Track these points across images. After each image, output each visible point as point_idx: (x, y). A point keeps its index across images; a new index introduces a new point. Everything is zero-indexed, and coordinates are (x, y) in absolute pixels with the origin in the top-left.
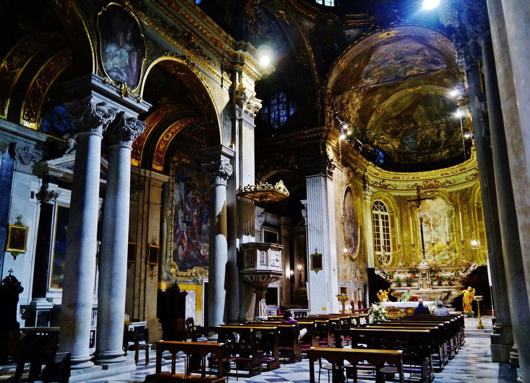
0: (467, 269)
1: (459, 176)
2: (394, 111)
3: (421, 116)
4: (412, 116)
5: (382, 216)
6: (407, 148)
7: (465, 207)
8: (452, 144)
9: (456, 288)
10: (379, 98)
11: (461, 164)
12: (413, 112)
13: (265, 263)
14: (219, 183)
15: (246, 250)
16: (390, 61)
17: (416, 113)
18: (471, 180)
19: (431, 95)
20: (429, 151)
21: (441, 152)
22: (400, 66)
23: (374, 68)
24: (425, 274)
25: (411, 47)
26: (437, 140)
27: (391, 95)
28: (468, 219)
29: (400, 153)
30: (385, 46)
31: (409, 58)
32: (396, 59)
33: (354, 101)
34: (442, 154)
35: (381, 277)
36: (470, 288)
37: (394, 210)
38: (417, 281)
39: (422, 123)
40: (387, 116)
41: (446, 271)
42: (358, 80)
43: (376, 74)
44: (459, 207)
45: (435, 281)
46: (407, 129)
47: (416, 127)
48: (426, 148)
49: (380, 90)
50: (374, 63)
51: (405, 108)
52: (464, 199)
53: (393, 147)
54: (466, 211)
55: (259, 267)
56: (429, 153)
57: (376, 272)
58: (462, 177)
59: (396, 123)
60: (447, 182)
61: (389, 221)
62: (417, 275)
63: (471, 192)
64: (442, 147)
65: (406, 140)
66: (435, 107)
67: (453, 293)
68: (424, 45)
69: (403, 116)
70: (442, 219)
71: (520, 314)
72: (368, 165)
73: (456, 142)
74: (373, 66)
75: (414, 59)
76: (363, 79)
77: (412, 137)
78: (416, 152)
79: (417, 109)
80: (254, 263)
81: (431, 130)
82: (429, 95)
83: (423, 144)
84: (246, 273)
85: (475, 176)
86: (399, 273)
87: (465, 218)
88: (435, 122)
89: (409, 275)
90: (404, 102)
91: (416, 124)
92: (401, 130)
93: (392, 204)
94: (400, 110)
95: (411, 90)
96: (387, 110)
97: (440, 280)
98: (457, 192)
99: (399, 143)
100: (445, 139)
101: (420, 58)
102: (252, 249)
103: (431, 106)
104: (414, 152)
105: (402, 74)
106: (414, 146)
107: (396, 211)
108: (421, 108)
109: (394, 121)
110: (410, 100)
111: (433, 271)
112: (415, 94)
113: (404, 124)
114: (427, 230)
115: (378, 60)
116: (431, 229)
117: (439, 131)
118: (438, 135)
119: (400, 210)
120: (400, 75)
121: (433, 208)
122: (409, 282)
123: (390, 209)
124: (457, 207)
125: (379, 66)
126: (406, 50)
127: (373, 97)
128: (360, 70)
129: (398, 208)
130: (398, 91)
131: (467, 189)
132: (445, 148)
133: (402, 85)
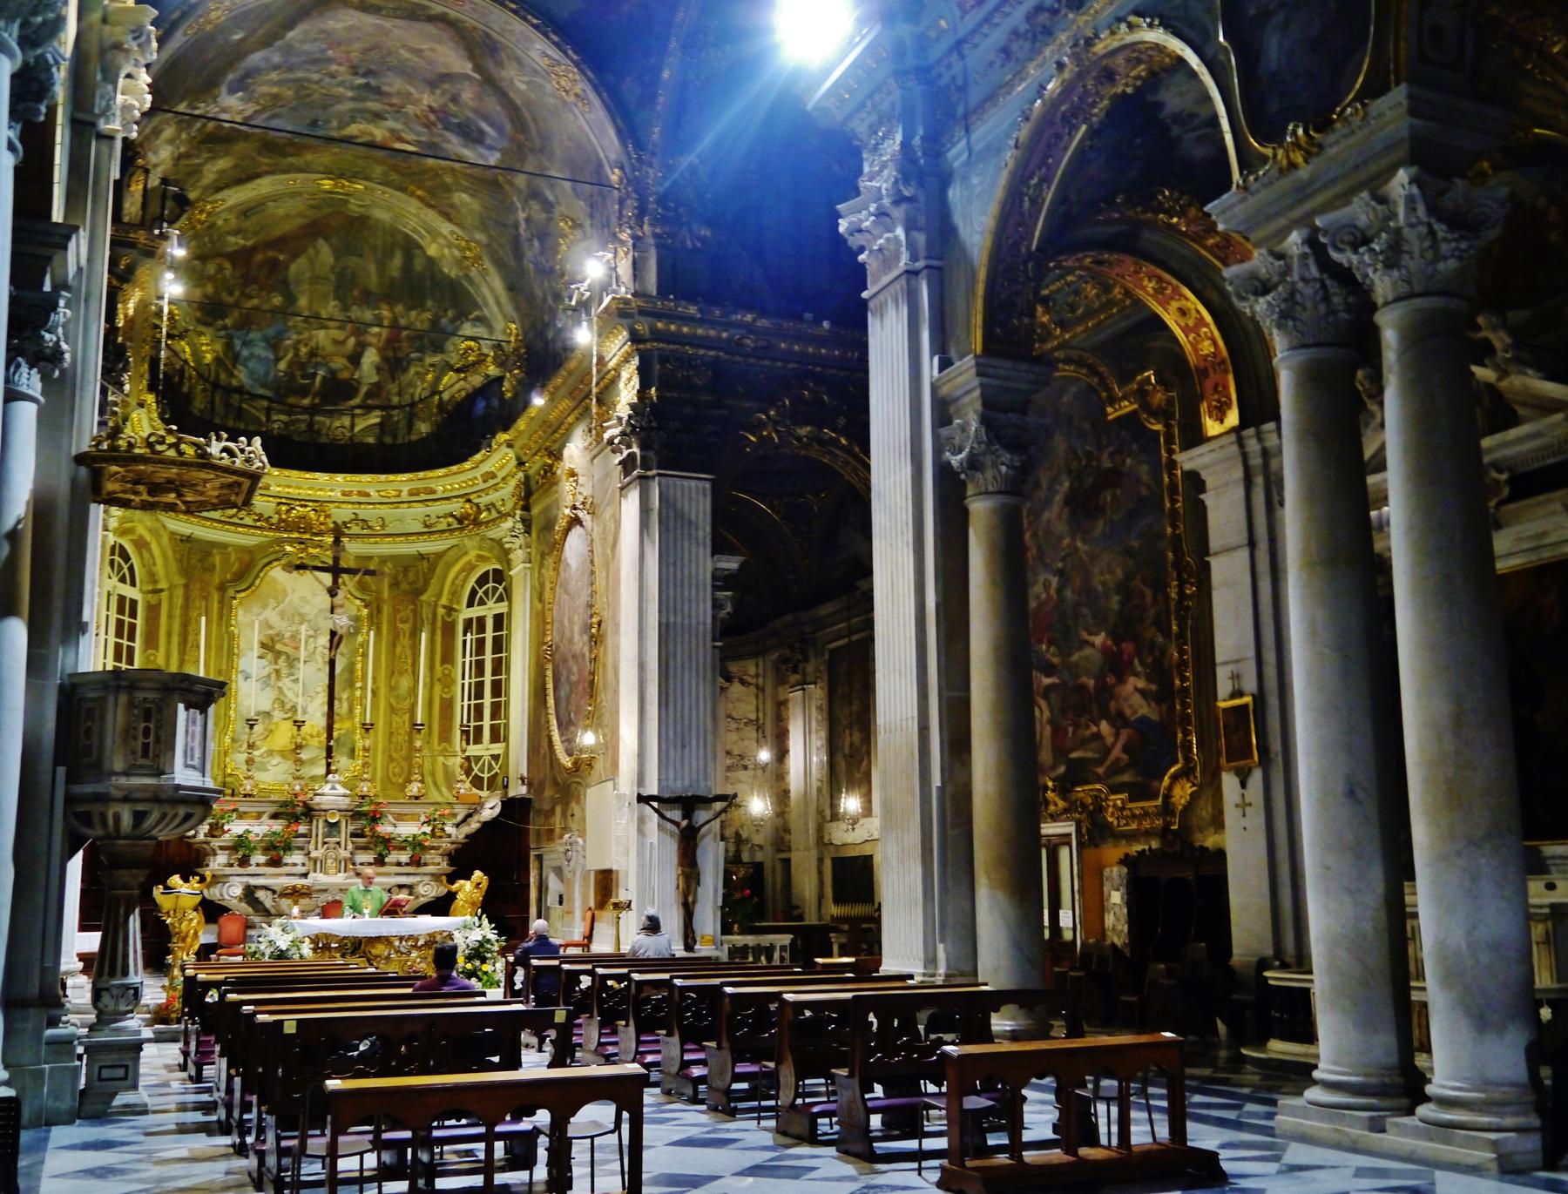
0: (470, 815)
1: (404, 510)
2: (237, 232)
3: (316, 279)
4: (287, 268)
5: (122, 599)
6: (242, 376)
7: (407, 612)
8: (395, 400)
9: (432, 875)
10: (221, 172)
11: (421, 474)
12: (295, 256)
13: (196, 762)
14: (24, 389)
15: (123, 698)
16: (334, 67)
17: (302, 262)
18: (443, 531)
19: (377, 220)
20: (313, 405)
21: (353, 416)
22: (350, 94)
23: (276, 67)
24: (336, 825)
25: (429, 54)
26: (345, 375)
27: (258, 176)
28: (409, 652)
29: (216, 385)
30: (357, 14)
31: (394, 84)
32: (354, 71)
33: (155, 153)
34: (353, 426)
36: (478, 874)
37: (163, 585)
38: (302, 848)
39: (311, 303)
40: (211, 241)
41: (400, 817)
42: (208, 87)
43: (264, 89)
44: (386, 609)
45: (365, 848)
46: (256, 308)
47: (287, 311)
48: (303, 391)
49: (240, 147)
50: (288, 50)
51: (276, 233)
52: (404, 586)
53: (196, 354)
54: (407, 627)
55: (183, 775)
56: (313, 410)
58: (412, 517)
59: (228, 273)
60: (356, 519)
61: (139, 622)
62: (302, 829)
63: (432, 569)
65: (245, 344)
66: (372, 268)
67: (421, 890)
68: (478, 68)
69: (259, 257)
71: (1474, 927)
72: (141, 405)
73: (407, 399)
74: (277, 59)
75: (409, 94)
76: (224, 89)
77: (266, 339)
78: (268, 393)
79: (311, 251)
80: (157, 756)
81: (339, 335)
82: (368, 218)
83: (298, 373)
84: (120, 794)
85: (460, 520)
86: (241, 816)
87: (399, 650)
88: (355, 312)
89: (278, 826)
90: (281, 212)
91: (291, 299)
92: (237, 305)
93: (159, 561)
94: (256, 234)
95: (327, 184)
96: (220, 222)
97: (387, 842)
99: (218, 347)
100: (375, 379)
101: (427, 99)
102: (150, 695)
103: (361, 256)
104: (261, 391)
105: (335, 123)
106: (267, 374)
107: (171, 588)
108: (324, 253)
109: (227, 265)
110: (301, 215)
111: (364, 817)
112: (329, 200)
113: (250, 290)
114: (265, 672)
115: (307, 47)
116: (277, 671)
117: (361, 347)
118: (355, 359)
119: (186, 586)
120: (328, 121)
121: (296, 600)
122: (276, 852)
123: (153, 578)
124: (379, 610)
125: (291, 69)
126: (405, 54)
127: (208, 160)
128: (240, 51)
129: (179, 581)
130: (286, 171)
131: (421, 557)
132: (368, 409)
133: (309, 157)
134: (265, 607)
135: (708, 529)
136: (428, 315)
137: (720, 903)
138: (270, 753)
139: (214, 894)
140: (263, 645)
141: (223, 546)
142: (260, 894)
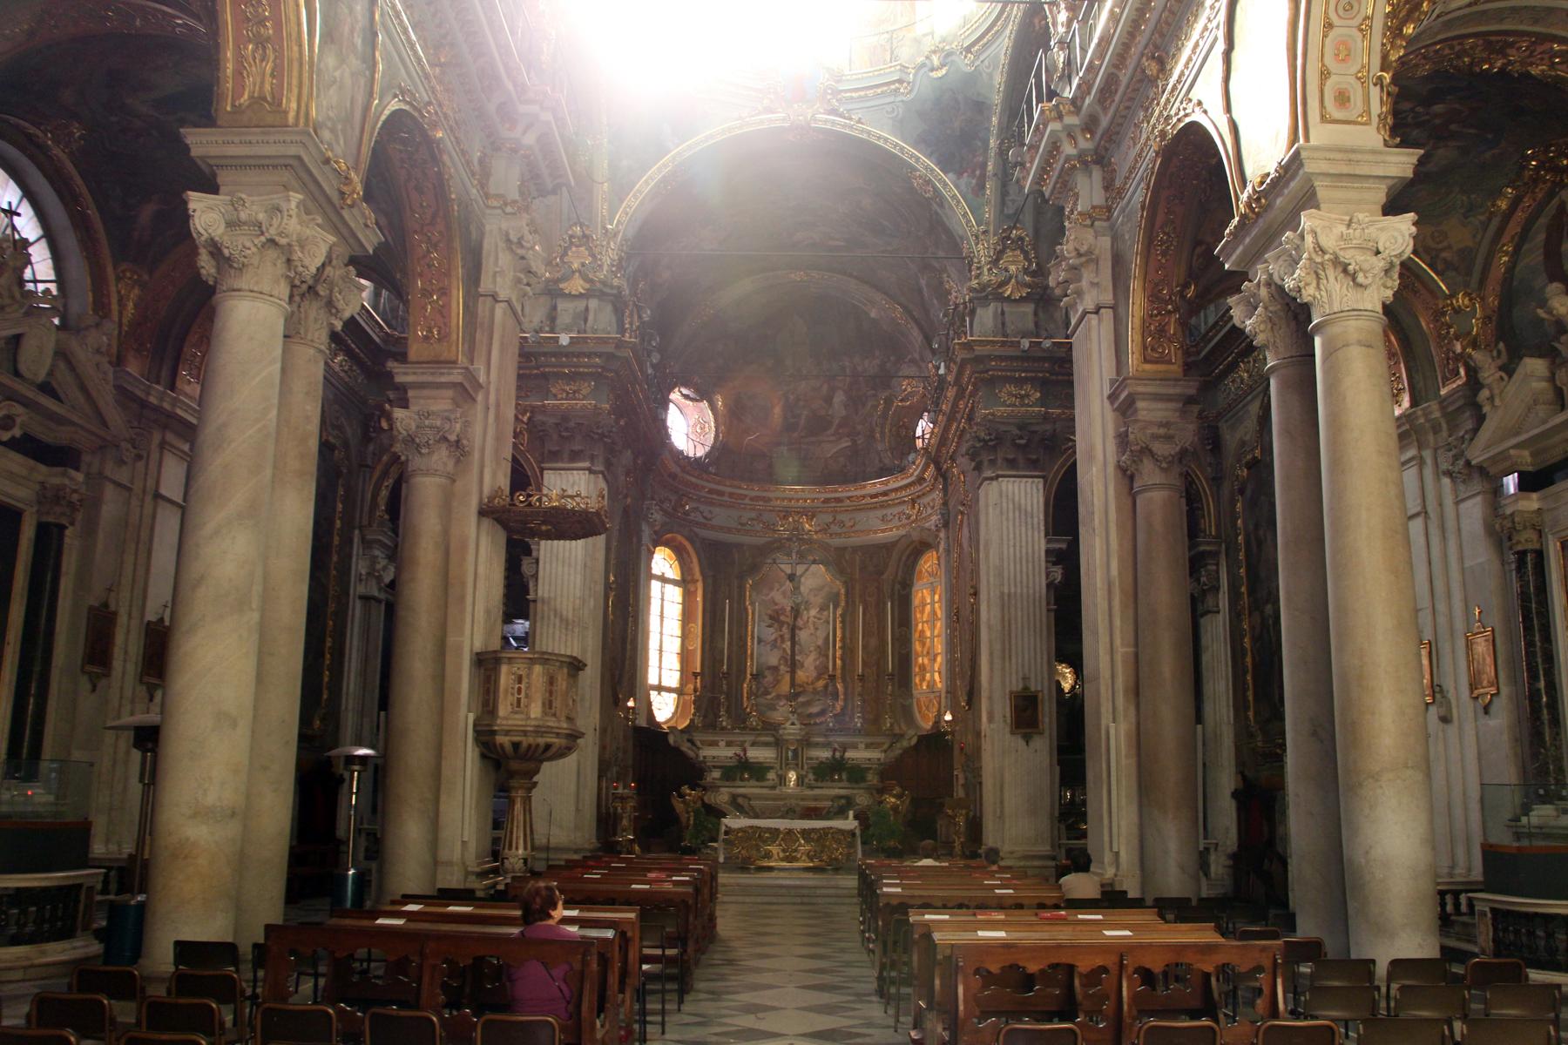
35: (682, 754)
57: (671, 740)
64: (832, 431)
70: (813, 612)
98: (855, 549)
100: (844, 413)
118: (828, 400)
134: (772, 589)
135: (1042, 517)
136: (877, 361)
137: (1057, 814)
138: (779, 697)
139: (710, 798)
140: (771, 617)
141: (739, 546)
142: (740, 800)
